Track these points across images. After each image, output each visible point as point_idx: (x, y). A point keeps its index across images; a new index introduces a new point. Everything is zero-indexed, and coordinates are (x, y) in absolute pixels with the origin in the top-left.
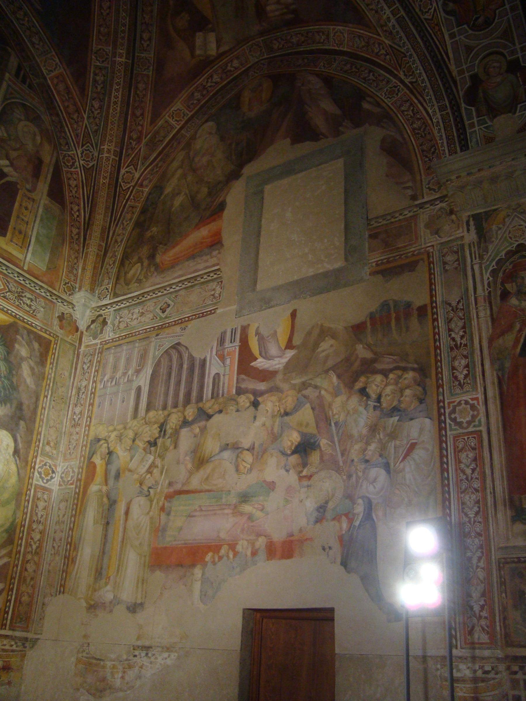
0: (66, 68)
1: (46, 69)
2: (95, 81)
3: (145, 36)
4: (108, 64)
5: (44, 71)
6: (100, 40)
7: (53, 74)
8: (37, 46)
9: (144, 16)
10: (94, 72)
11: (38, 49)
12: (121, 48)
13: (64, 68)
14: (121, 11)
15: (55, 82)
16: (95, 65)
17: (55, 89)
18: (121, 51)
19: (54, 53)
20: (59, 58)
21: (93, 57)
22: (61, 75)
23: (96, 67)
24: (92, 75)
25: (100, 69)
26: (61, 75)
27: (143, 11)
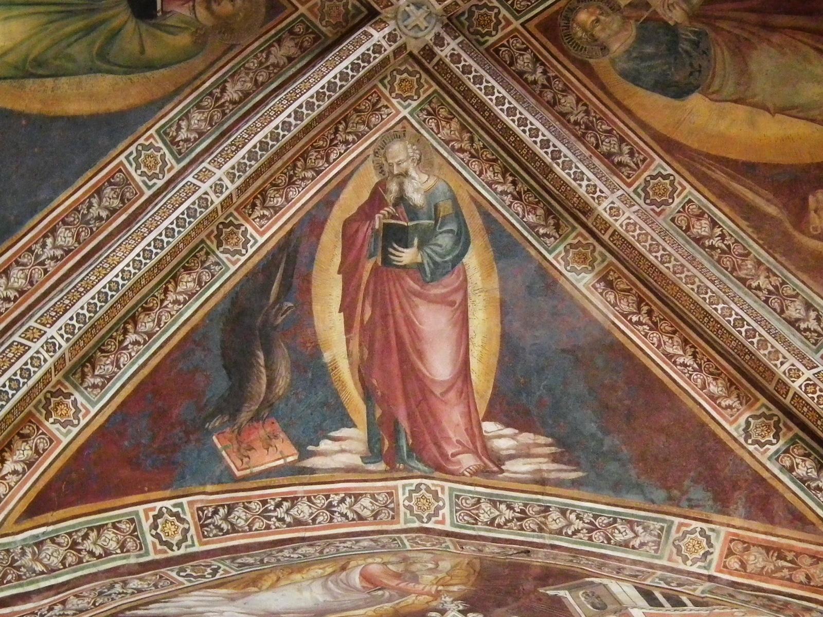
0: (724, 519)
1: (694, 562)
2: (803, 481)
3: (795, 310)
4: (790, 429)
5: (694, 569)
6: (730, 407)
7: (715, 557)
8: (636, 543)
9: (754, 284)
10: (783, 468)
11: (642, 544)
12: (778, 363)
13: (722, 524)
14: (708, 308)
15: (737, 566)
16: (770, 459)
17: (750, 576)
18: (786, 366)
19: (677, 520)
20: (695, 519)
21: (751, 448)
22: (732, 541)
23: (776, 457)
24: (785, 478)
25: (787, 451)
26: (733, 540)
27: (743, 281)
